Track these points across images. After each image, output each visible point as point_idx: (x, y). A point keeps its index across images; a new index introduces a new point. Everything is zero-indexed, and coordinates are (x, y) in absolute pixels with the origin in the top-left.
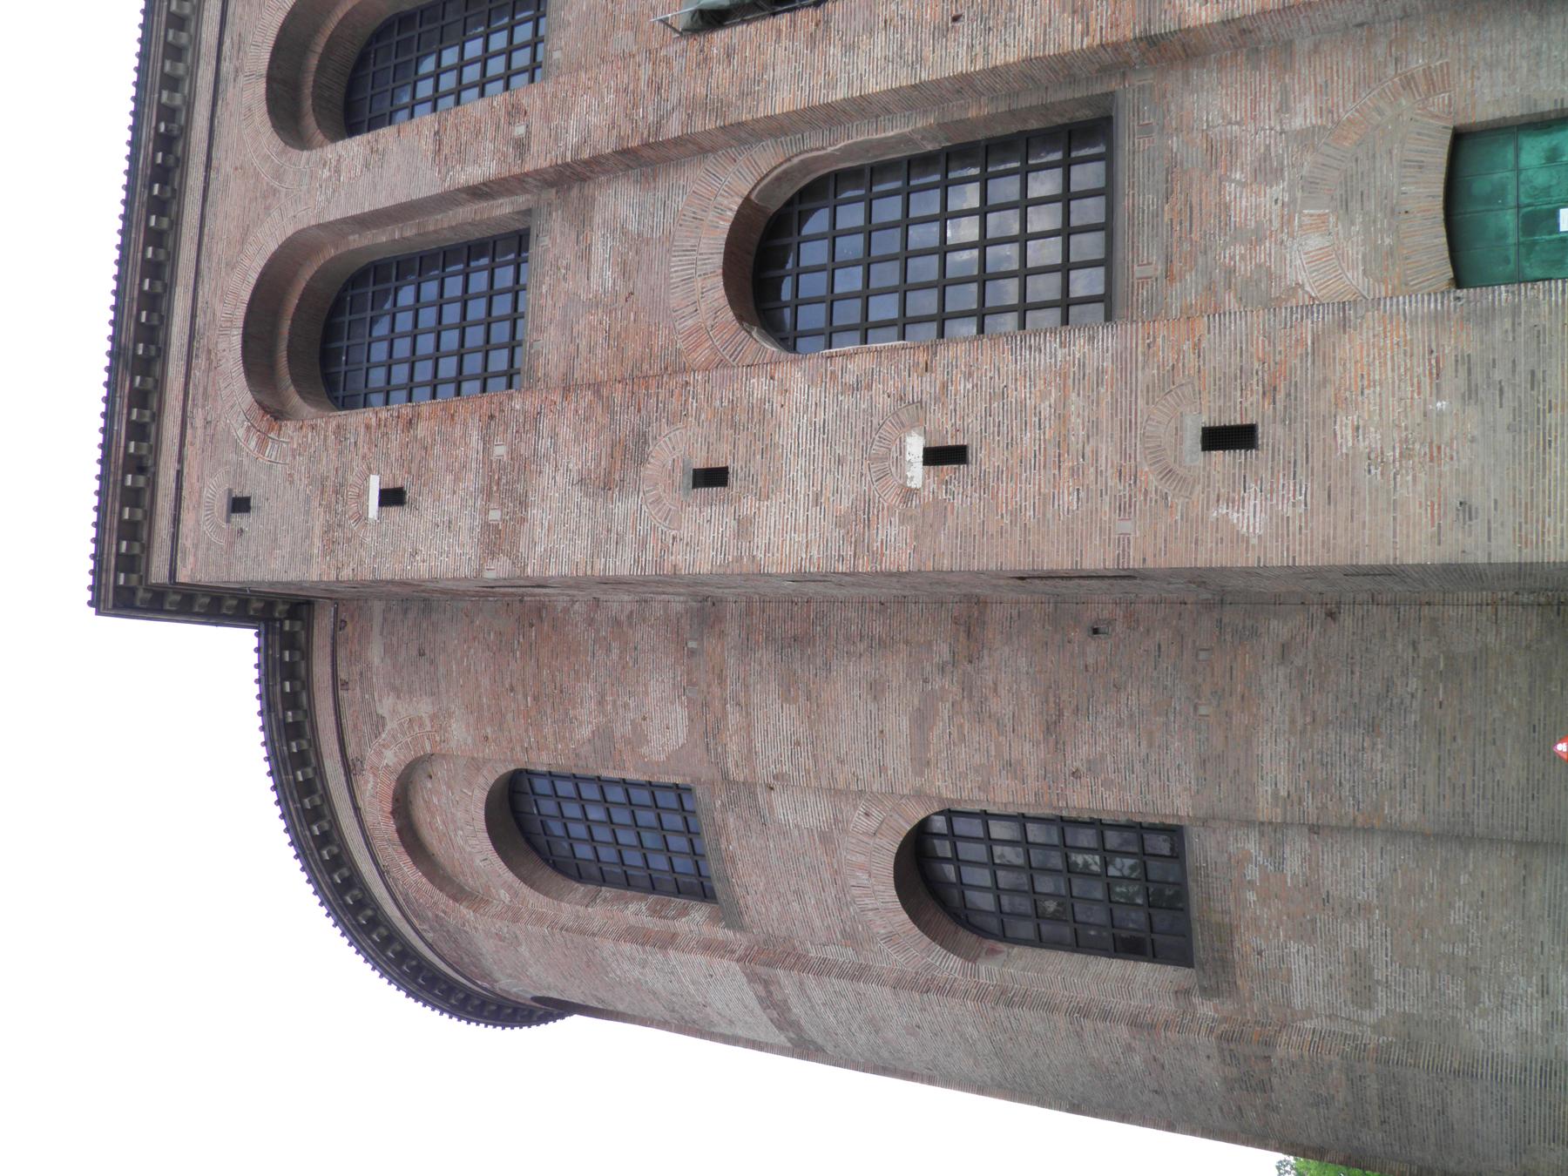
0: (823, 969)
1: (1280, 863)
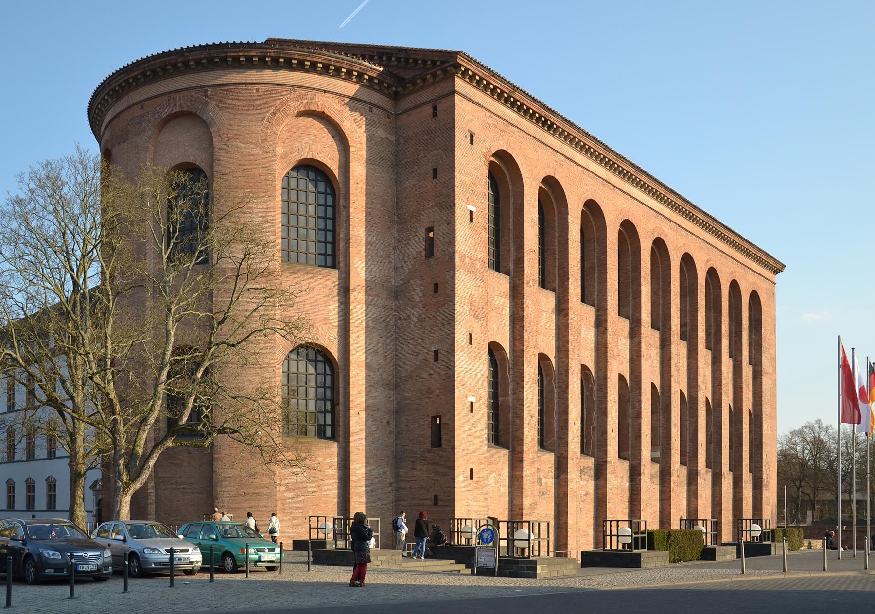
1: (331, 468)
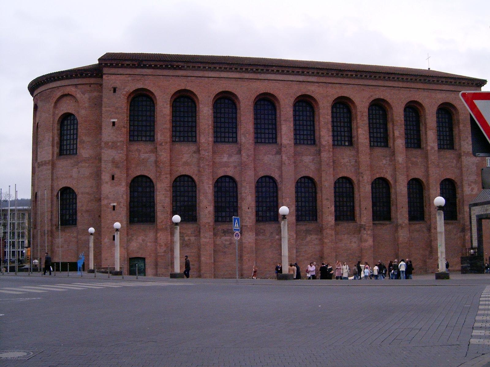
0: (52, 173)
1: (73, 238)
